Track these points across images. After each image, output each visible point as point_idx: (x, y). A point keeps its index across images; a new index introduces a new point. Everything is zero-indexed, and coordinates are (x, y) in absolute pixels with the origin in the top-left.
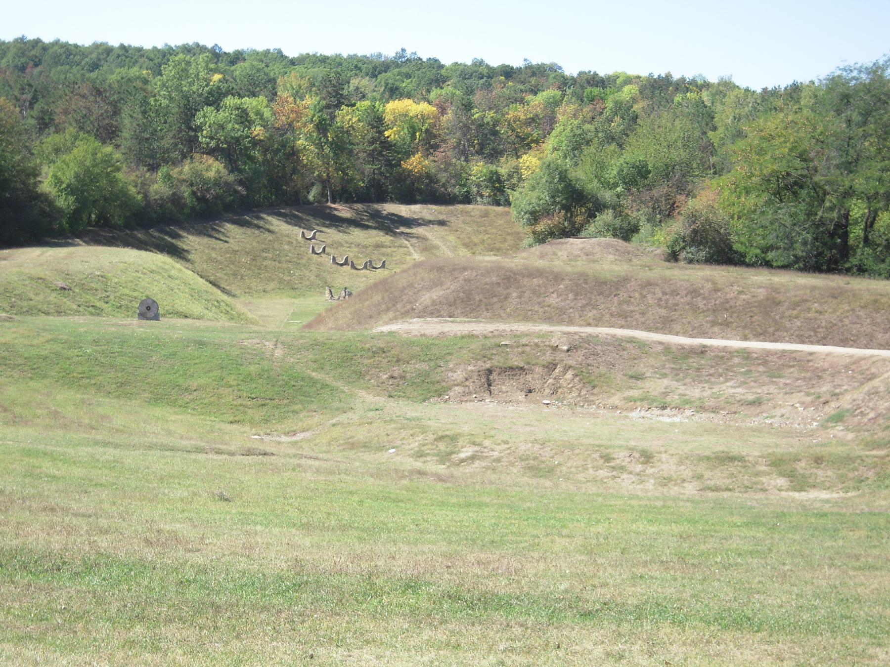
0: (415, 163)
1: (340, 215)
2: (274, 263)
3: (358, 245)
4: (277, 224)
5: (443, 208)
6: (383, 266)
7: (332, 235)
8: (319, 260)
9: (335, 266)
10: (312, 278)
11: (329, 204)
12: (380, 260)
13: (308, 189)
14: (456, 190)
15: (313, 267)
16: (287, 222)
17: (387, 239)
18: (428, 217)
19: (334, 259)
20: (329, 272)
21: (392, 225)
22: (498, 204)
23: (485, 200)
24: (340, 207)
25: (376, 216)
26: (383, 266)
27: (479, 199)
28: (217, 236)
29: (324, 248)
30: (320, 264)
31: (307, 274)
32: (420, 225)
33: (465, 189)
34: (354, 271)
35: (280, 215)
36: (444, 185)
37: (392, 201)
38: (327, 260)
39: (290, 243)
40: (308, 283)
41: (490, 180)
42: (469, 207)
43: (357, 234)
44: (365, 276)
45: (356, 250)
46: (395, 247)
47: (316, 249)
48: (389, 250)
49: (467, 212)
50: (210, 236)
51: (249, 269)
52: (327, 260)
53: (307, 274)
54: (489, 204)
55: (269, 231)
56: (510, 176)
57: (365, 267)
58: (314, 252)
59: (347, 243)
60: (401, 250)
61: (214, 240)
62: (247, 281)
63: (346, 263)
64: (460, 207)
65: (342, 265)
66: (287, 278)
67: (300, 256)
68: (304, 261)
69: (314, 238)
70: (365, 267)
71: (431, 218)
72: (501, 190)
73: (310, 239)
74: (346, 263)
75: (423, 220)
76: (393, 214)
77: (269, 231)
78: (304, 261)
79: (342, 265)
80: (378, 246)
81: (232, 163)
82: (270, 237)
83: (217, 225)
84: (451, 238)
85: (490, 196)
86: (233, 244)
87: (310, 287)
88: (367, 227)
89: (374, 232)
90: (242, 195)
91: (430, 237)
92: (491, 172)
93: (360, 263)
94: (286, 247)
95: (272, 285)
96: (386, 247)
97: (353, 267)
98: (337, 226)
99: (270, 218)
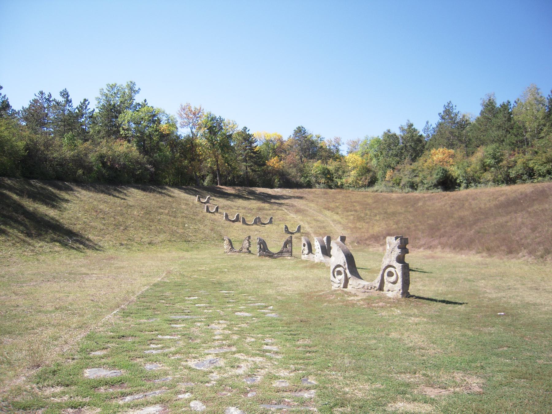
0: (273, 162)
1: (226, 191)
2: (168, 217)
3: (245, 208)
4: (177, 192)
5: (296, 190)
6: (271, 222)
7: (222, 202)
8: (213, 217)
9: (228, 222)
10: (207, 231)
11: (218, 186)
12: (266, 219)
13: (203, 177)
14: (302, 180)
15: (207, 222)
16: (186, 193)
17: (266, 206)
18: (288, 194)
19: (227, 216)
20: (223, 227)
21: (265, 198)
22: (331, 188)
23: (322, 185)
24: (226, 188)
25: (252, 193)
26: (271, 222)
27: (317, 185)
28: (117, 195)
29: (217, 208)
30: (214, 220)
31: (202, 227)
32: (284, 198)
33: (308, 179)
34: (245, 226)
35: (180, 188)
36: (293, 177)
37: (259, 187)
38: (220, 218)
39: (186, 204)
40: (202, 236)
41: (323, 173)
42: (313, 190)
43: (240, 202)
44: (256, 230)
45: (244, 211)
46: (274, 210)
47: (210, 209)
48: (270, 212)
49: (312, 192)
50: (110, 194)
51: (139, 221)
52: (220, 218)
53: (202, 227)
54: (324, 188)
55: (170, 196)
56: (337, 170)
57: (255, 223)
58: (208, 210)
59: (235, 206)
60: (280, 212)
61: (112, 197)
62: (132, 231)
63: (237, 220)
64: (307, 190)
65: (234, 221)
66: (180, 231)
67: (196, 214)
68: (199, 218)
69: (208, 202)
70: (255, 223)
71: (291, 195)
72: (331, 179)
73: (205, 203)
74: (237, 220)
76: (264, 193)
77: (170, 196)
78: (199, 218)
79: (234, 221)
80: (260, 209)
81: (143, 149)
82: (170, 199)
83: (121, 188)
84: (312, 205)
85: (324, 183)
86: (131, 201)
87: (206, 239)
88: (249, 199)
89: (254, 202)
90: (151, 172)
91: (296, 205)
92: (323, 168)
93: (251, 219)
94: (183, 207)
95: (162, 237)
96: (266, 210)
97: (244, 222)
98: (225, 198)
99: (172, 189)
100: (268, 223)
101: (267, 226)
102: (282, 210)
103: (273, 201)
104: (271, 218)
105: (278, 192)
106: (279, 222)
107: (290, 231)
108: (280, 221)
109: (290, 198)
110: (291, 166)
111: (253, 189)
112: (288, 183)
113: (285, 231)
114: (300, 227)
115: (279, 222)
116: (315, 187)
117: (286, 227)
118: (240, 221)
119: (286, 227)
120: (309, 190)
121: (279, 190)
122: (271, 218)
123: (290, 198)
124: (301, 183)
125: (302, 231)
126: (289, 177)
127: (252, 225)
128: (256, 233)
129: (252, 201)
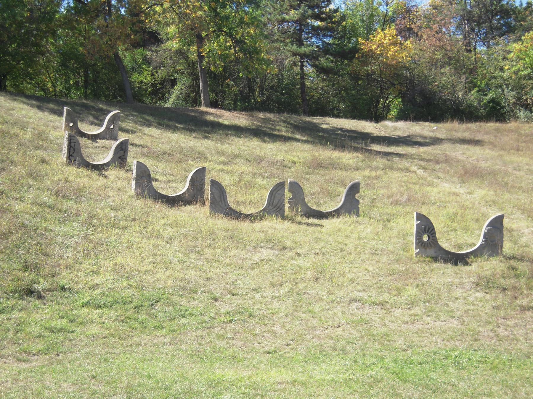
6: (351, 205)
11: (203, 108)
14: (473, 96)
27: (522, 113)
33: (491, 95)
34: (223, 223)
44: (270, 242)
49: (510, 131)
57: (274, 207)
59: (220, 153)
65: (172, 202)
70: (274, 207)
75: (425, 138)
88: (287, 139)
89: (307, 147)
100: (337, 213)
101: (328, 224)
102: (407, 170)
103: (376, 148)
104: (354, 188)
105: (396, 129)
106: (390, 210)
107: (445, 245)
108: (396, 203)
109: (435, 141)
110: (438, 56)
111: (317, 120)
112: (426, 105)
113: (420, 244)
114: (497, 225)
115: (390, 210)
116: (517, 118)
117: (426, 227)
118: (203, 203)
119: (426, 227)
120: (498, 125)
121: (401, 124)
122: (354, 188)
123: (435, 141)
124: (469, 106)
125: (507, 247)
126: (433, 87)
127: (259, 217)
128: (267, 253)
129: (296, 144)
